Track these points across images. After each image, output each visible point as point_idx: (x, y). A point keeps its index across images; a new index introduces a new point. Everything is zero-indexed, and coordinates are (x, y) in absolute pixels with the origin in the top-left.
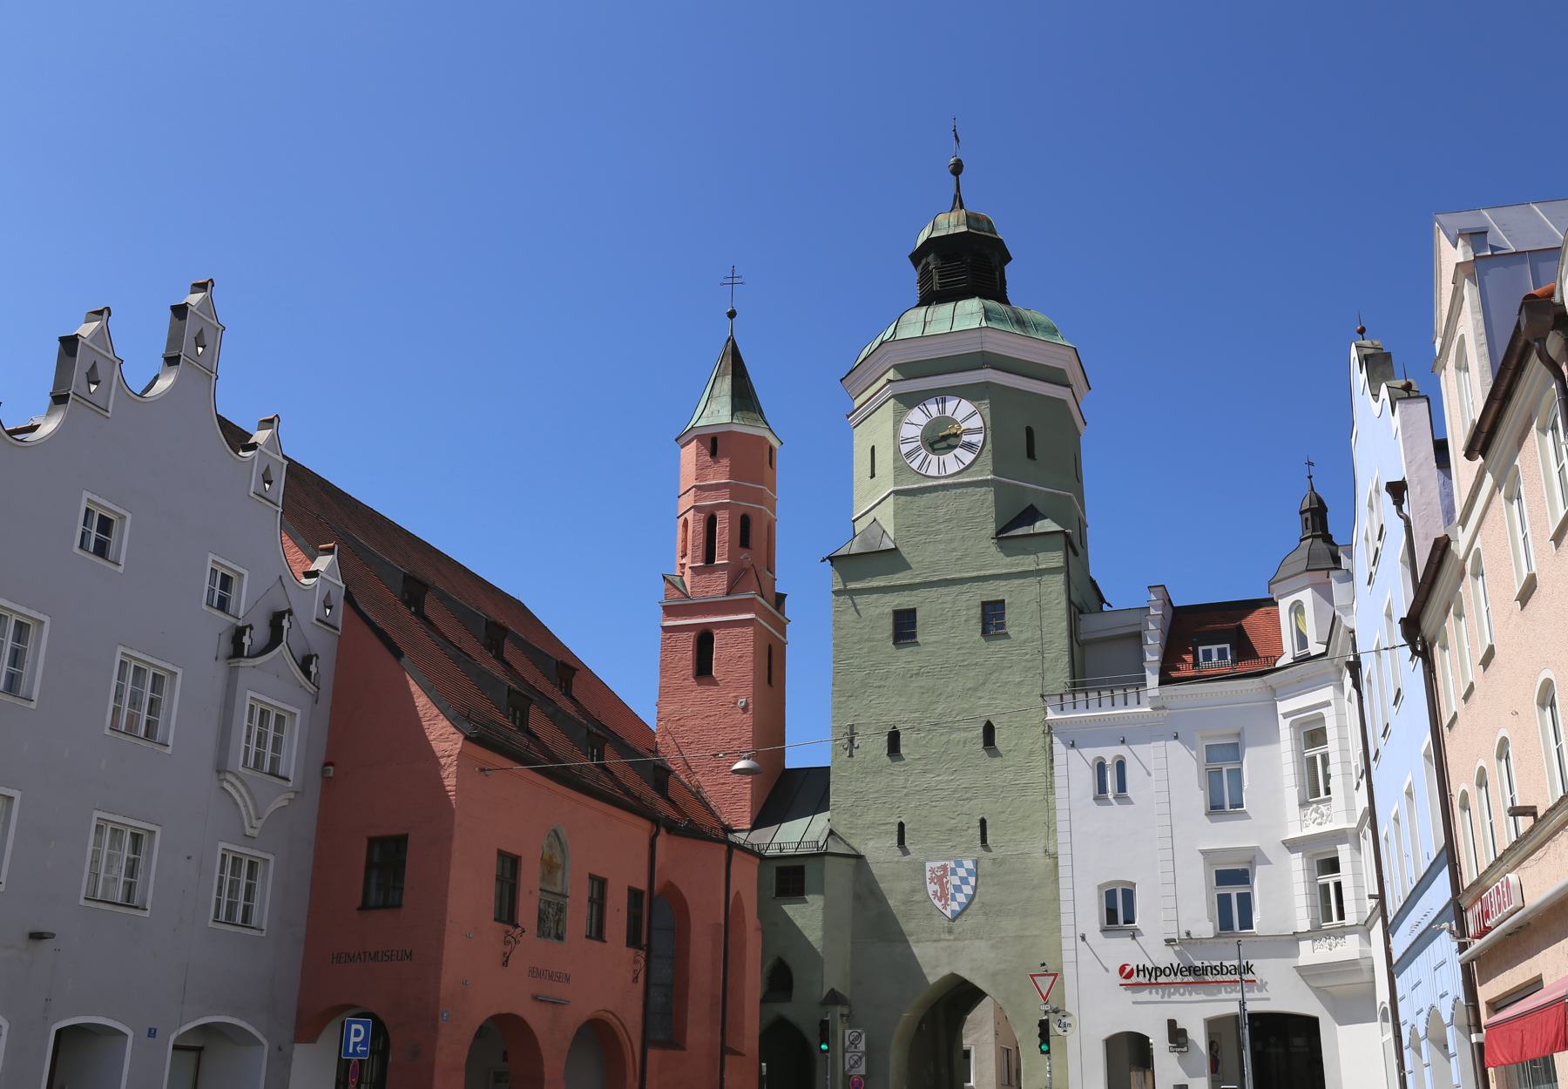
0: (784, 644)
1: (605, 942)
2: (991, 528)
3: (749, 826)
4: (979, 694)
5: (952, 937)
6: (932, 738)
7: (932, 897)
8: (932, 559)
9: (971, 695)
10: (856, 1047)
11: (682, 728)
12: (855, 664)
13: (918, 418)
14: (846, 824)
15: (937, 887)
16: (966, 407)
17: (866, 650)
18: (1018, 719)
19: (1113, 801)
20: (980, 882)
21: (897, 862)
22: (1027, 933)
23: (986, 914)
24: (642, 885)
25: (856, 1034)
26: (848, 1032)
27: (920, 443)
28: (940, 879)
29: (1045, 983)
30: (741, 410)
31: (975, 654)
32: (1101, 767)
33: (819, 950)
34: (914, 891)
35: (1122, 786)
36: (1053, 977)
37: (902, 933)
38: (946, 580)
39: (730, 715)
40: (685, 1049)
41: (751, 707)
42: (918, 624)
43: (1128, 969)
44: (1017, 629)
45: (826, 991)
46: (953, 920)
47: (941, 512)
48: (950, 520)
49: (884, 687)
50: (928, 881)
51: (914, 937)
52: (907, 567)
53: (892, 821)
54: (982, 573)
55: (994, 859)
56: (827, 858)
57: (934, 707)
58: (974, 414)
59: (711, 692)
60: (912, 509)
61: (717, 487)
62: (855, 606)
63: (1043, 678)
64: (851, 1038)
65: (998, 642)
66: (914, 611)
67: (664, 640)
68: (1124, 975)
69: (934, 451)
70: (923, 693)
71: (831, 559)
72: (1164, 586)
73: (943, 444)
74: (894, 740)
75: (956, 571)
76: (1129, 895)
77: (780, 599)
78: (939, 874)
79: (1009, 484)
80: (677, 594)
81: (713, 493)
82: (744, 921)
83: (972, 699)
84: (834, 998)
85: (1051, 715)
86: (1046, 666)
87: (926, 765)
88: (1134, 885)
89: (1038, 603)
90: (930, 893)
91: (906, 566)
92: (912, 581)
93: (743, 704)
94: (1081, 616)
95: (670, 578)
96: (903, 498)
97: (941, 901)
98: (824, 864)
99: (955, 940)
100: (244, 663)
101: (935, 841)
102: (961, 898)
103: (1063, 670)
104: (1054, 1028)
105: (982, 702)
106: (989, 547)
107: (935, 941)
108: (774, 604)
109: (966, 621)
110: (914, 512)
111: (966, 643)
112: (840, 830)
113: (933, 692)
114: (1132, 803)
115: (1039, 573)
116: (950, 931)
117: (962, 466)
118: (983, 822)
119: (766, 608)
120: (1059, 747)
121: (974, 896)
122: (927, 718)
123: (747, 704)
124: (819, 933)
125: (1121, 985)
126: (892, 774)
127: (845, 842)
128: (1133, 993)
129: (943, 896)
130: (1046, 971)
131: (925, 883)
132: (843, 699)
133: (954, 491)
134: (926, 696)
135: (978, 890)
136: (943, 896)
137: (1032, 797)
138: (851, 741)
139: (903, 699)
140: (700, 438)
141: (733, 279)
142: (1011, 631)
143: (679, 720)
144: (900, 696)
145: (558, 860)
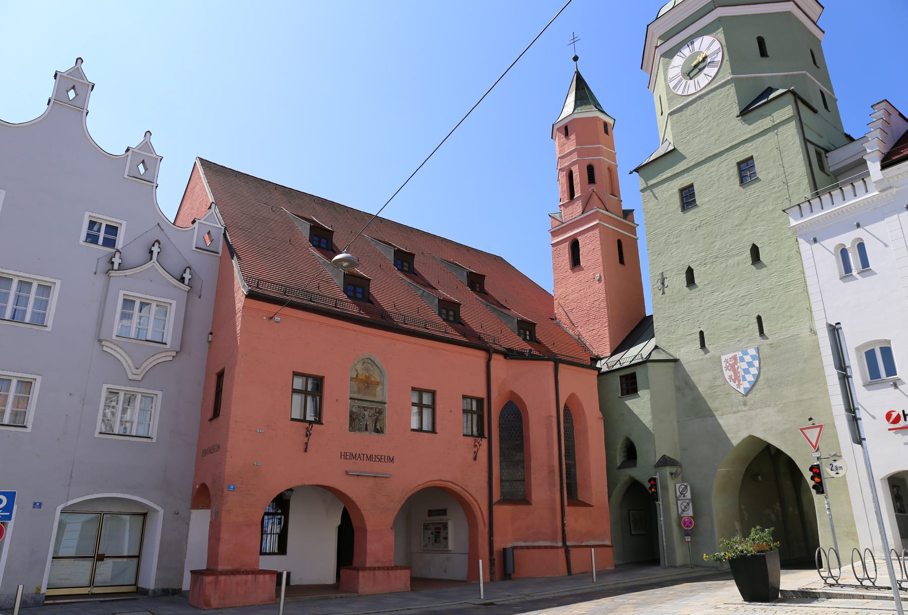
0: (635, 241)
1: (437, 433)
2: (736, 111)
3: (609, 354)
4: (744, 227)
5: (747, 408)
6: (714, 268)
7: (728, 380)
8: (699, 148)
9: (738, 230)
10: (684, 496)
11: (567, 302)
12: (660, 232)
13: (678, 61)
14: (666, 340)
15: (731, 373)
16: (707, 39)
17: (664, 221)
18: (775, 236)
19: (858, 276)
20: (762, 364)
21: (702, 360)
22: (805, 397)
23: (770, 387)
24: (482, 394)
25: (683, 486)
26: (678, 486)
27: (681, 77)
28: (733, 366)
29: (813, 434)
30: (581, 106)
31: (737, 200)
32: (844, 253)
33: (650, 429)
34: (715, 378)
35: (865, 263)
36: (819, 428)
37: (710, 411)
38: (710, 157)
39: (592, 286)
40: (531, 504)
41: (603, 278)
42: (696, 193)
43: (894, 415)
44: (764, 172)
45: (658, 457)
46: (746, 395)
47: (701, 115)
48: (707, 117)
49: (679, 241)
50: (724, 369)
51: (719, 412)
52: (683, 158)
53: (695, 331)
54: (734, 143)
55: (770, 344)
56: (649, 364)
57: (713, 245)
58: (713, 41)
59: (580, 275)
60: (682, 120)
61: (570, 153)
62: (654, 195)
63: (790, 201)
64: (681, 490)
65: (752, 186)
66: (692, 186)
67: (553, 252)
68: (891, 420)
69: (691, 79)
70: (705, 238)
71: (636, 170)
72: (886, 100)
73: (696, 70)
74: (690, 273)
75: (716, 149)
76: (887, 352)
77: (628, 214)
78: (731, 363)
79: (747, 78)
80: (557, 223)
81: (568, 158)
82: (584, 413)
83: (739, 232)
84: (665, 461)
85: (793, 223)
86: (791, 191)
87: (713, 287)
88: (889, 342)
89: (778, 149)
90: (727, 378)
91: (683, 158)
92: (688, 166)
93: (598, 278)
94: (827, 155)
95: (553, 215)
96: (675, 116)
97: (735, 383)
98: (648, 369)
99: (750, 410)
100: (113, 273)
101: (726, 339)
102: (750, 378)
103: (805, 190)
104: (827, 471)
105: (747, 232)
106: (737, 124)
107: (735, 412)
108: (622, 215)
109: (728, 179)
110: (683, 121)
111: (730, 194)
112: (662, 345)
113: (712, 236)
114: (876, 274)
115: (775, 127)
116: (745, 404)
117: (710, 79)
118: (759, 319)
119: (611, 217)
120: (804, 245)
121: (759, 374)
122: (710, 254)
123: (600, 277)
124: (650, 417)
125: (889, 430)
126: (691, 299)
127: (666, 352)
128: (903, 435)
129: (736, 378)
130: (813, 424)
131: (722, 371)
132: (655, 257)
133: (707, 97)
134: (707, 239)
135: (762, 370)
136: (736, 378)
137: (794, 291)
138: (663, 283)
139: (693, 246)
140: (558, 129)
141: (574, 40)
142: (759, 175)
143: (566, 297)
144: (690, 244)
145: (376, 377)
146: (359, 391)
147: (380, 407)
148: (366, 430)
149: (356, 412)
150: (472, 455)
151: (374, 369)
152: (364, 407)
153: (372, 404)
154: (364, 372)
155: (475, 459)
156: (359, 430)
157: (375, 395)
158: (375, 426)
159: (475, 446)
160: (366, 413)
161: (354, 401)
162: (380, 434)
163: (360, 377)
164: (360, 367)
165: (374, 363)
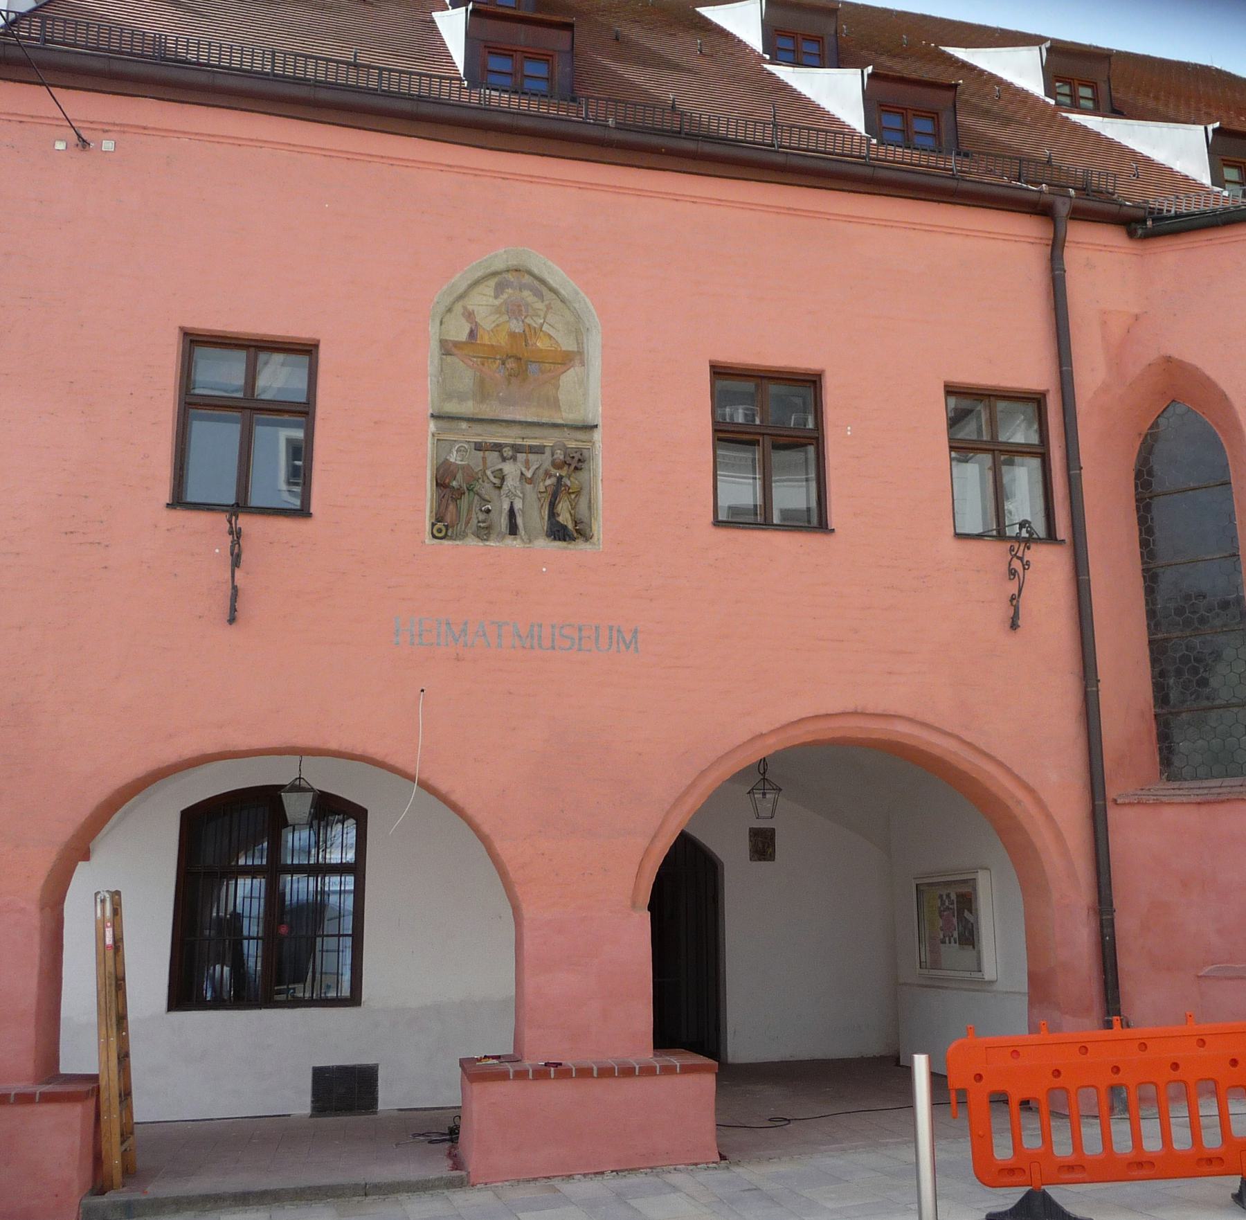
146: (482, 391)
147: (572, 445)
148: (513, 530)
149: (463, 467)
150: (1002, 612)
151: (549, 307)
152: (498, 447)
153: (537, 432)
154: (506, 318)
155: (1014, 625)
156: (484, 532)
157: (555, 404)
158: (553, 514)
159: (1012, 573)
160: (508, 468)
161: (454, 424)
162: (572, 546)
163: (485, 339)
164: (483, 302)
165: (543, 282)
